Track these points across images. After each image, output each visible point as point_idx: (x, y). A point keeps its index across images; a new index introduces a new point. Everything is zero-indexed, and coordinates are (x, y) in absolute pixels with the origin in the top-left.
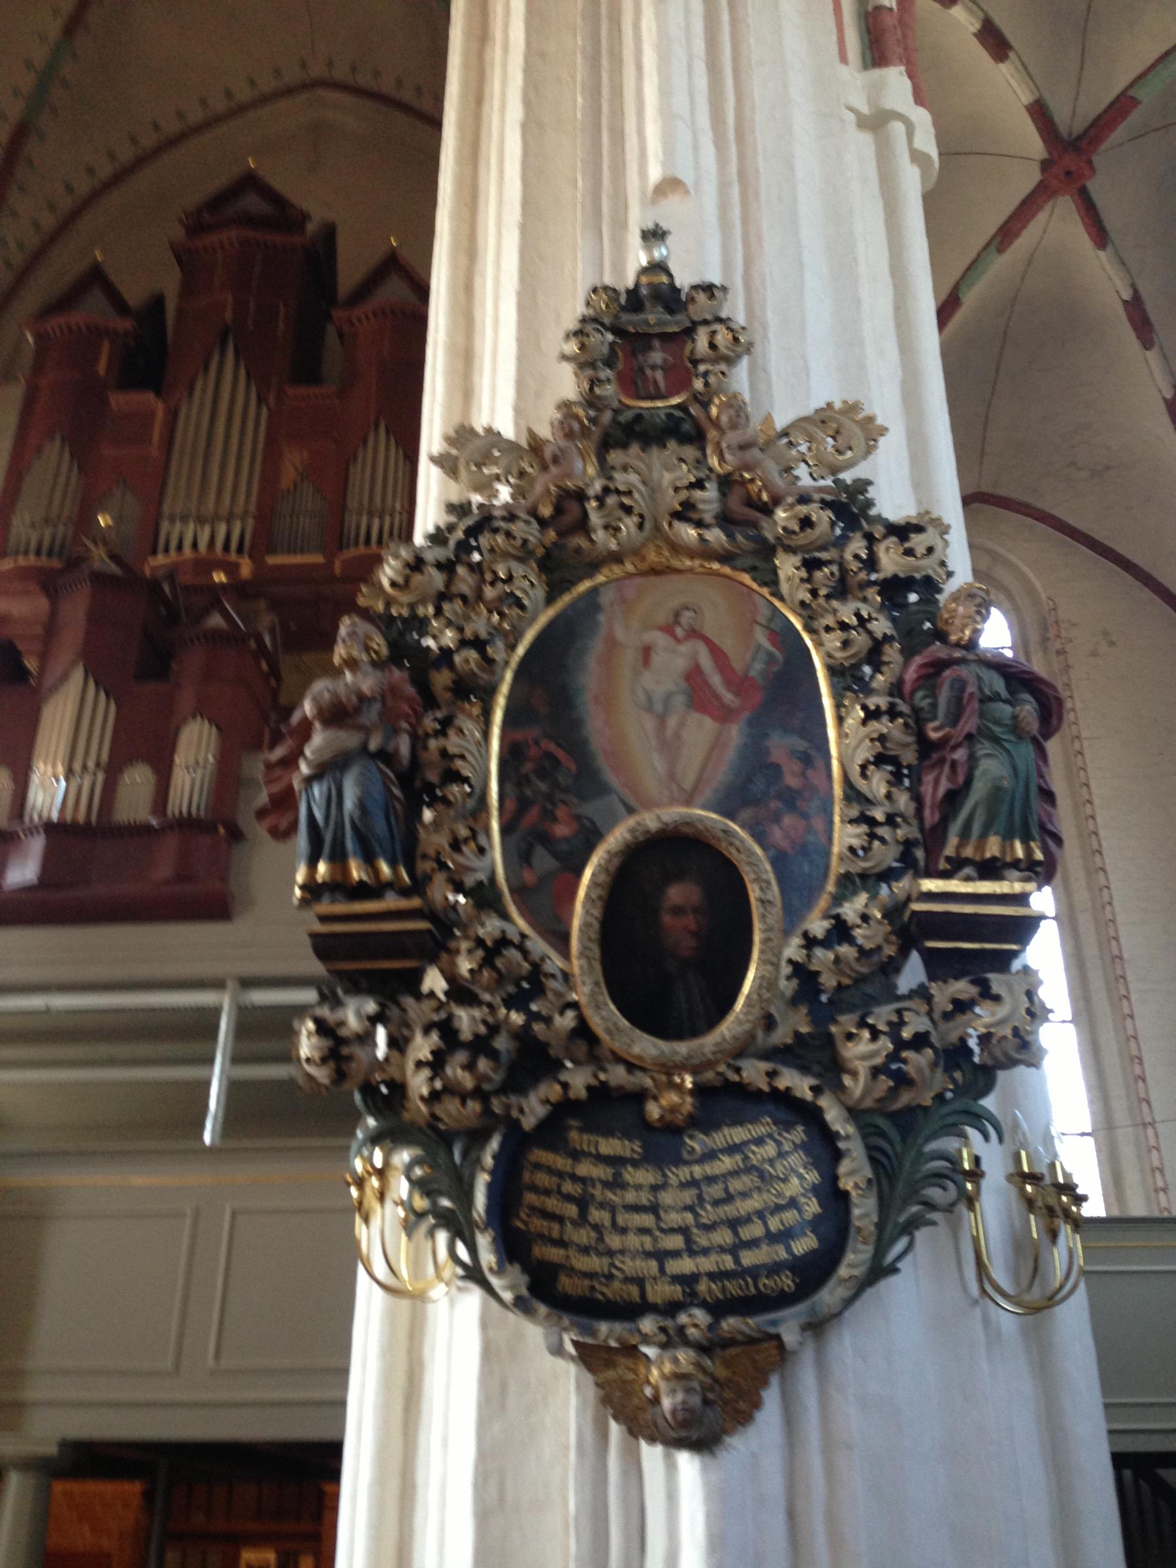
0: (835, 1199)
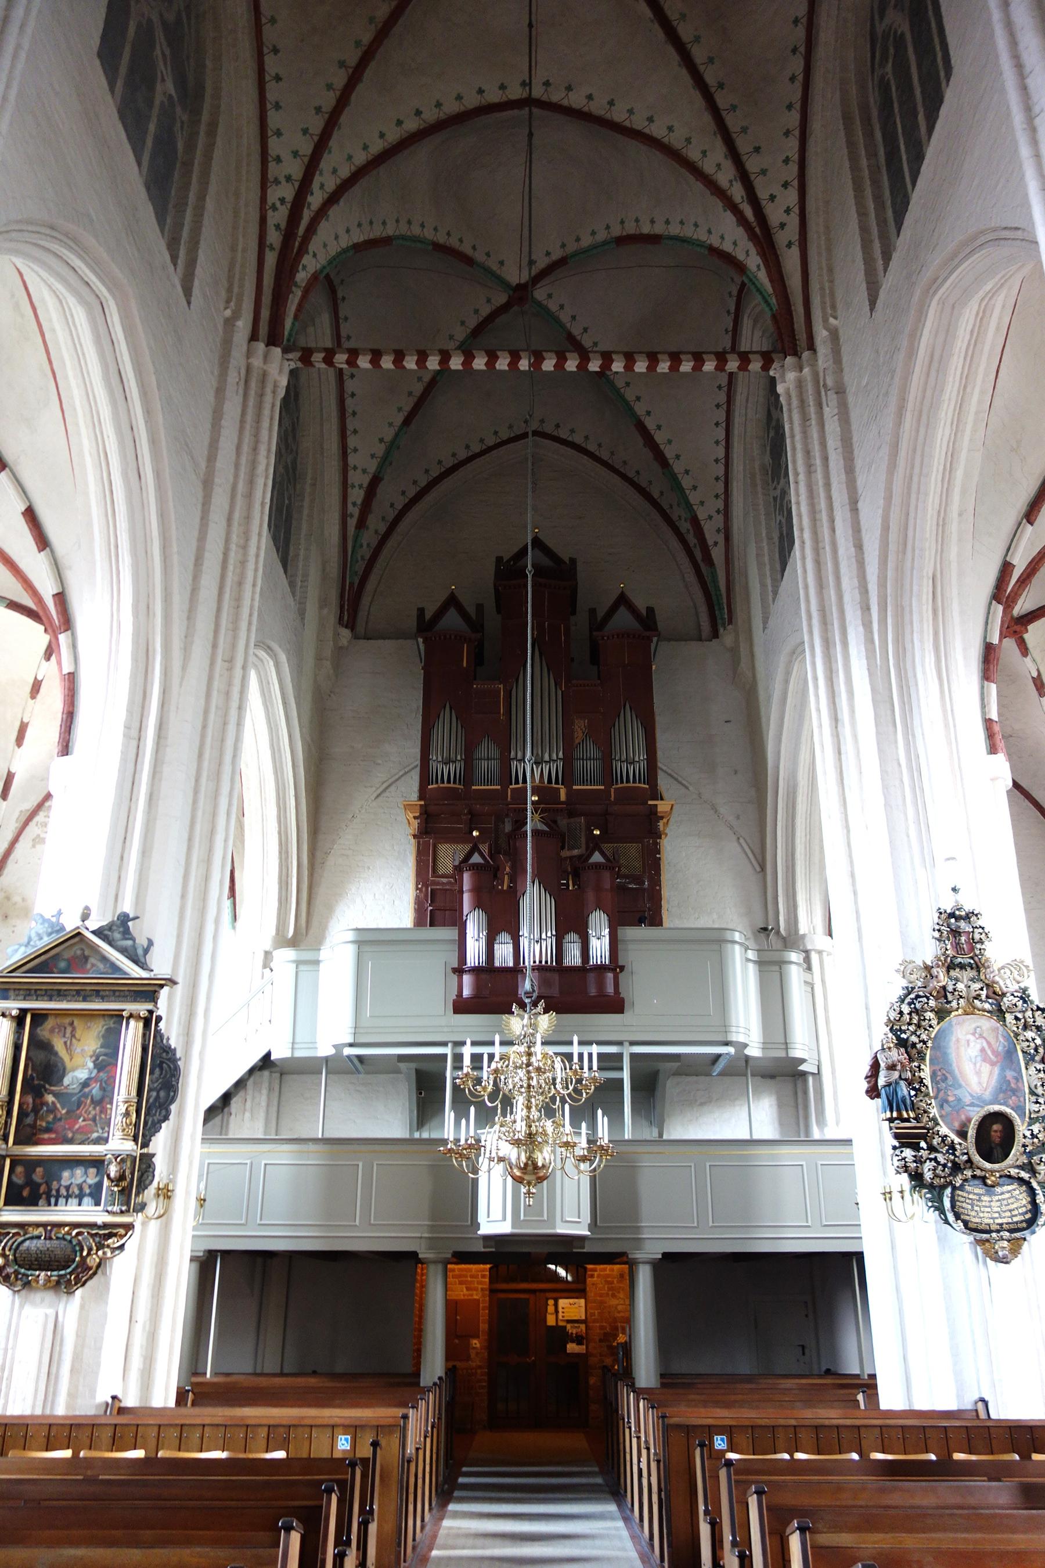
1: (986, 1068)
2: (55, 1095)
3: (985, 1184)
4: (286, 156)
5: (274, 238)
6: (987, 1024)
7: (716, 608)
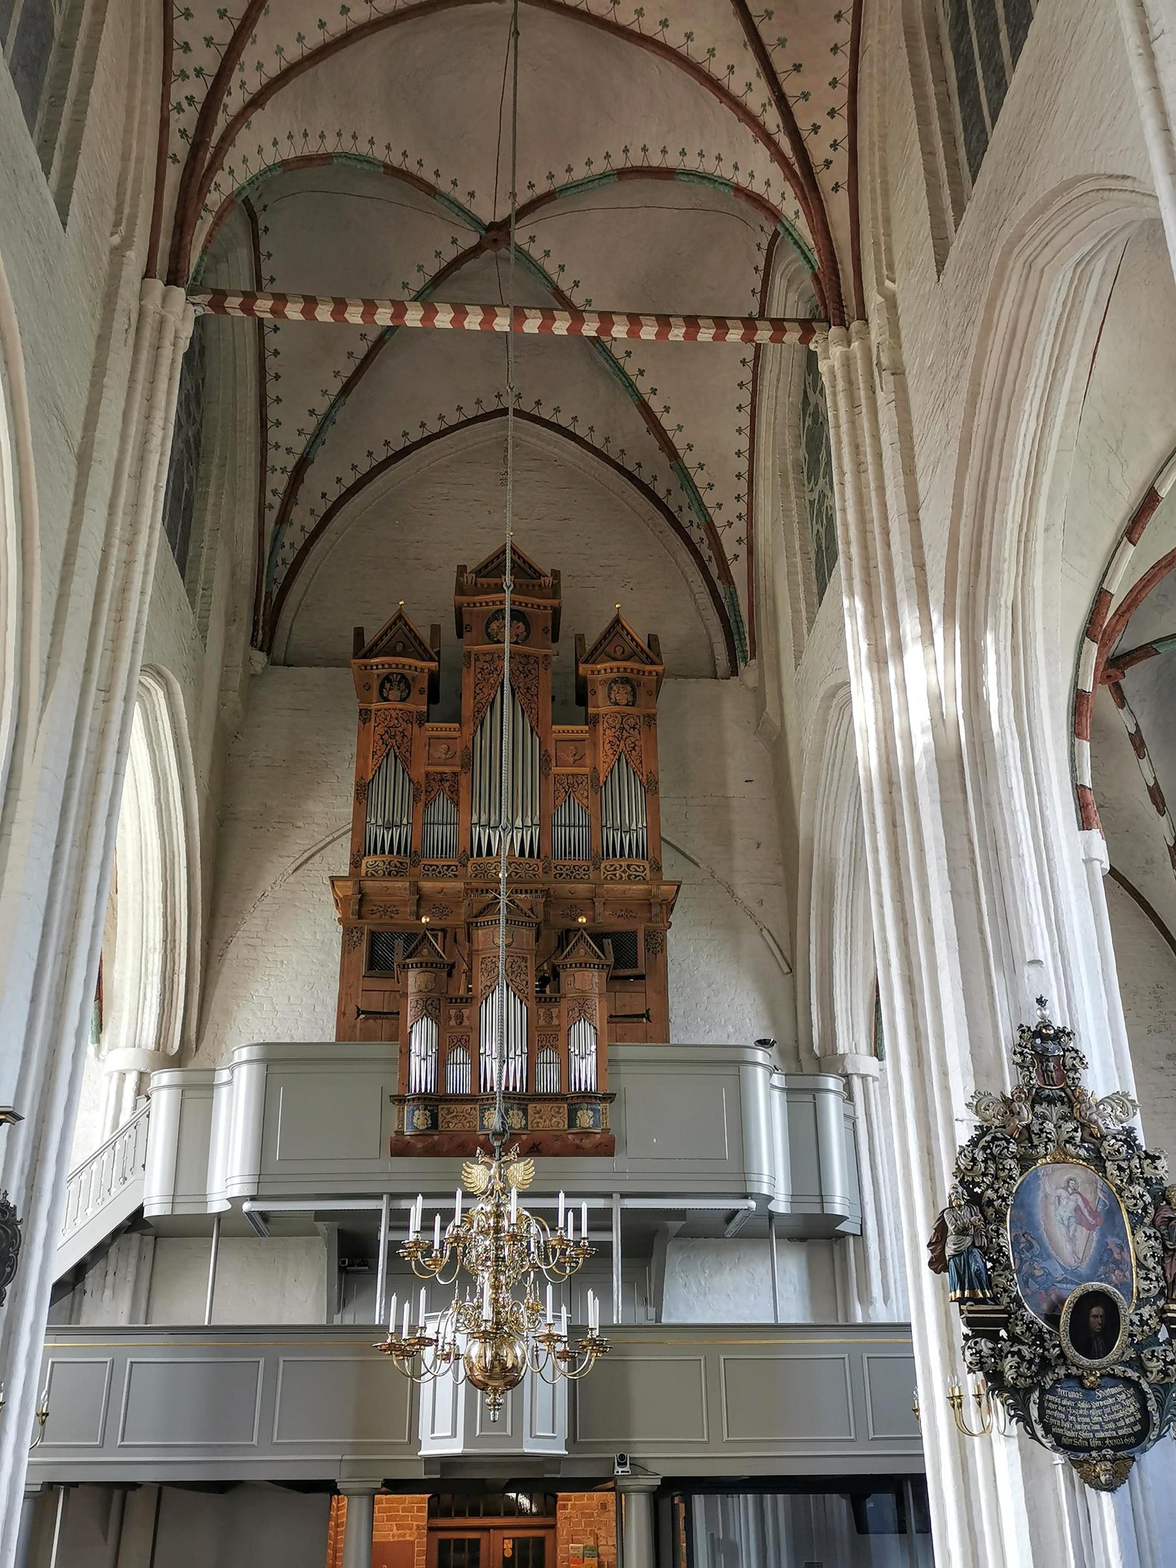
0: (1144, 1410)
1: (1082, 1233)
3: (1083, 1386)
4: (197, 44)
5: (179, 146)
6: (1081, 1174)
7: (736, 637)
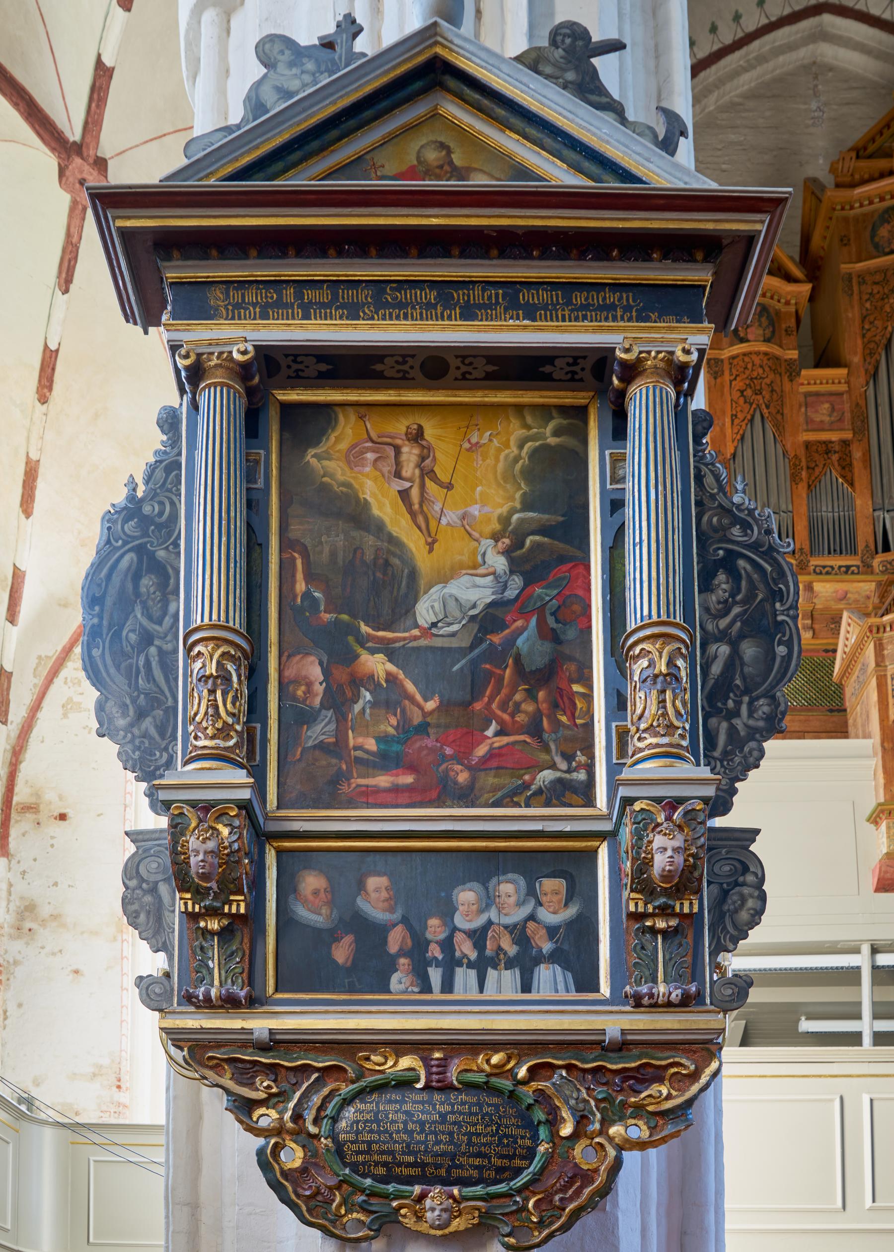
2: (391, 655)
